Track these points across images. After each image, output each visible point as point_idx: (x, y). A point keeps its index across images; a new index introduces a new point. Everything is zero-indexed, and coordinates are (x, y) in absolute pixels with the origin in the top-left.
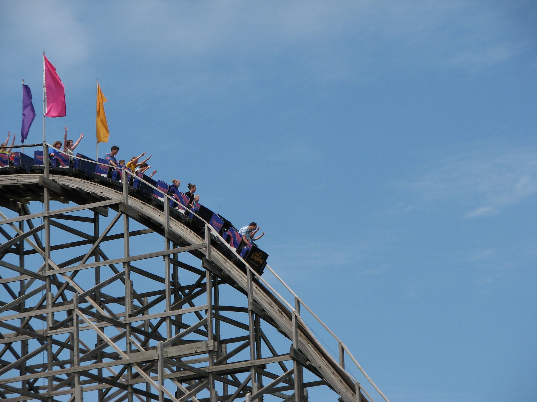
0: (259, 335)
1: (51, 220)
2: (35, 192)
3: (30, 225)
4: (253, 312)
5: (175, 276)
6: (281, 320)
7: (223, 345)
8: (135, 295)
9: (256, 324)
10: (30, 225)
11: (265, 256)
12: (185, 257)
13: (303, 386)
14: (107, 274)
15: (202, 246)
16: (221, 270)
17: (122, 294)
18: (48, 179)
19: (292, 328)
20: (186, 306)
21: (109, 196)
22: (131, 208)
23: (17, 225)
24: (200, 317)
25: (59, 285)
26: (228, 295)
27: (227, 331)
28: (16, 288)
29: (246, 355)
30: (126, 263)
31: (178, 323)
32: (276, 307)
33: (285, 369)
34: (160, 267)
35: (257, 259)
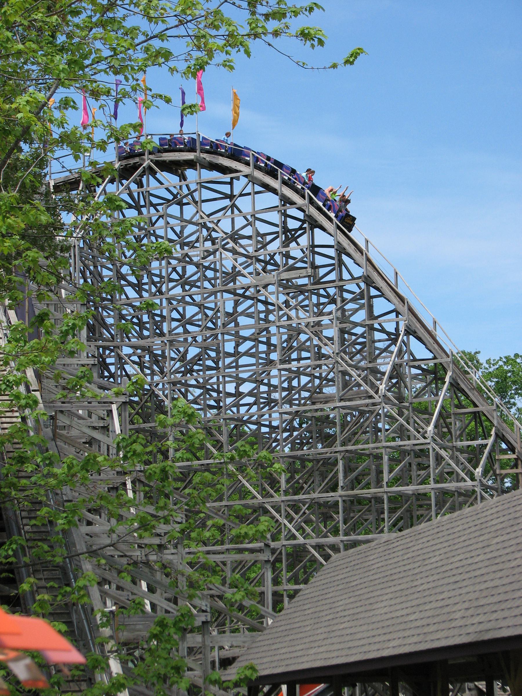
0: (341, 263)
1: (201, 185)
2: (191, 164)
3: (189, 189)
4: (337, 250)
5: (285, 222)
6: (356, 255)
7: (317, 270)
8: (258, 234)
9: (339, 256)
10: (189, 189)
11: (354, 219)
12: (292, 211)
13: (371, 297)
14: (240, 222)
15: (303, 205)
16: (316, 221)
17: (250, 234)
18: (200, 157)
19: (362, 260)
20: (293, 244)
21: (241, 169)
22: (256, 178)
23: (178, 187)
24: (304, 252)
25: (208, 229)
26: (320, 237)
27: (319, 260)
28: (178, 229)
29: (332, 276)
30: (253, 216)
31: (287, 256)
32: (353, 247)
33: (360, 288)
34: (275, 217)
35: (348, 221)
